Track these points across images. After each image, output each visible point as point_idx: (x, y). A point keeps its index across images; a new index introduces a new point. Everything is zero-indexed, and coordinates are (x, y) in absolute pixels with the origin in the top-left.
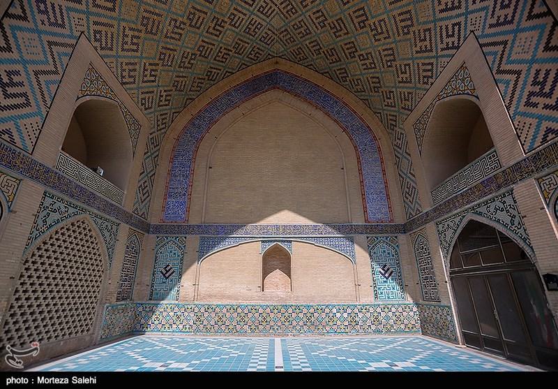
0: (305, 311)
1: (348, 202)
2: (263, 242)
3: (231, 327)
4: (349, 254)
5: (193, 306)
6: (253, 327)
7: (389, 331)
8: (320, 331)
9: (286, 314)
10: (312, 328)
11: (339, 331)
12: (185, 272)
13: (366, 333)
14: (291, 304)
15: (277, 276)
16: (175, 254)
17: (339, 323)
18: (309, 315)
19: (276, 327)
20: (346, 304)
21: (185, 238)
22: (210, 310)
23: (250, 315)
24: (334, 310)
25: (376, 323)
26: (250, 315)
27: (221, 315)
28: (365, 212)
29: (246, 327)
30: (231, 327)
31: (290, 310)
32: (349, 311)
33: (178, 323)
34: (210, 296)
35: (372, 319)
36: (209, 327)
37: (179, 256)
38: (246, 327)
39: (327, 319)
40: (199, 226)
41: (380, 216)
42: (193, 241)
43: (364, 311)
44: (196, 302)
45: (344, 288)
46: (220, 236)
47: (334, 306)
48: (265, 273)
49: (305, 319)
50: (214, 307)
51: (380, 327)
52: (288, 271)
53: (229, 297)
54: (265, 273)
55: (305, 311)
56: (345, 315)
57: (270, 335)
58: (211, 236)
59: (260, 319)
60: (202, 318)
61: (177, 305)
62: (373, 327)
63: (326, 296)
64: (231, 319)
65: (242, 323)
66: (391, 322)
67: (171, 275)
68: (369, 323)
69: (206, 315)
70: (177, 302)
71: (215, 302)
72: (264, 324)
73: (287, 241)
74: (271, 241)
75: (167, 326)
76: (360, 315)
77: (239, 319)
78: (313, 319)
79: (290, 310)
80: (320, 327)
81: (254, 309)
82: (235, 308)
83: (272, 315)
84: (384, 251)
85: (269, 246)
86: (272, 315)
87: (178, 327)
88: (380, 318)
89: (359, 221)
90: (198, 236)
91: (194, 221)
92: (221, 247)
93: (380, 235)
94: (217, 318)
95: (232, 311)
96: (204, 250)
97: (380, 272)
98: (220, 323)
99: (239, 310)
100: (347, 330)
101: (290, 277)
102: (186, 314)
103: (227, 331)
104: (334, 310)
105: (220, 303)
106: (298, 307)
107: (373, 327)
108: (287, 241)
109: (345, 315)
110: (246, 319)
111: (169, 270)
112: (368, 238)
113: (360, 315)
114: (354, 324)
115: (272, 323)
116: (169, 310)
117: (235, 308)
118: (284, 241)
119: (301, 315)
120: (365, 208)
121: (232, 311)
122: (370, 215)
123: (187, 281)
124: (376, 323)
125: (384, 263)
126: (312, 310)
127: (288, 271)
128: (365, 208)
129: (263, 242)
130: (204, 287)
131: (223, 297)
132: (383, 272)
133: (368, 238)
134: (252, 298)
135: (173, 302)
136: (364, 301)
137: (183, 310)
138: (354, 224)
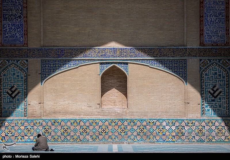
0: (138, 124)
1: (185, 25)
2: (101, 64)
3: (75, 137)
4: (181, 75)
5: (41, 121)
6: (94, 137)
7: (210, 141)
8: (151, 140)
9: (123, 127)
10: (144, 137)
11: (167, 140)
12: (31, 90)
13: (190, 142)
14: (126, 118)
15: (114, 94)
16: (18, 76)
17: (167, 134)
18: (142, 127)
19: (113, 137)
20: (175, 118)
21: (27, 61)
22: (56, 124)
23: (91, 128)
24: (164, 124)
25: (200, 134)
26: (91, 128)
27: (66, 127)
28: (201, 35)
29: (88, 137)
30: (75, 137)
31: (126, 124)
32: (177, 124)
33: (29, 135)
34: (55, 112)
35: (197, 131)
36: (56, 137)
37: (22, 78)
38: (88, 137)
39: (157, 131)
40: (38, 50)
41: (214, 39)
42: (35, 64)
43: (190, 124)
44: (43, 118)
45: (175, 105)
46: (59, 59)
47: (164, 120)
48: (104, 90)
49: (138, 131)
50: (60, 121)
51: (204, 138)
52: (124, 89)
53: (72, 113)
54: (104, 90)
55: (138, 124)
56: (174, 128)
57: (108, 142)
58: (54, 59)
59: (100, 130)
60: (50, 131)
61: (27, 121)
62: (197, 138)
63: (158, 112)
64: (75, 131)
65: (85, 134)
66: (214, 134)
67: (18, 95)
68: (193, 134)
69: (53, 128)
70: (26, 118)
71: (60, 117)
72: (104, 134)
73: (124, 63)
74: (109, 63)
75: (20, 137)
76: (186, 128)
77: (81, 130)
78: (145, 130)
79: (126, 124)
80: (151, 137)
81: (94, 122)
82: (78, 121)
83: (110, 127)
84: (216, 73)
85: (107, 67)
86: (110, 127)
87: (29, 138)
88: (204, 131)
89: (193, 44)
90: (39, 59)
91: (33, 44)
92: (63, 69)
93: (213, 58)
94: (62, 131)
95: (75, 124)
96: (46, 72)
97: (209, 92)
98: (65, 134)
99: (82, 124)
100: (174, 140)
101: (126, 94)
102: (35, 127)
103: (72, 140)
104: (164, 124)
105: (64, 118)
106: (132, 121)
107: (197, 138)
108: (124, 63)
109: (174, 128)
110: (88, 131)
111: (15, 91)
112: (201, 60)
113: (186, 128)
114: (180, 135)
115: (110, 134)
116: (19, 125)
117: (78, 121)
118: (121, 63)
119: (135, 128)
120: (201, 30)
121: (75, 124)
122: (206, 38)
123: (33, 100)
124: (200, 134)
125: (214, 84)
126: (145, 123)
127: (124, 89)
128: (201, 30)
129: (101, 64)
130: (49, 104)
131: (66, 113)
132: (212, 92)
133: (201, 60)
134: (92, 114)
135: (23, 118)
136: (191, 116)
137: (32, 124)
138: (189, 47)
